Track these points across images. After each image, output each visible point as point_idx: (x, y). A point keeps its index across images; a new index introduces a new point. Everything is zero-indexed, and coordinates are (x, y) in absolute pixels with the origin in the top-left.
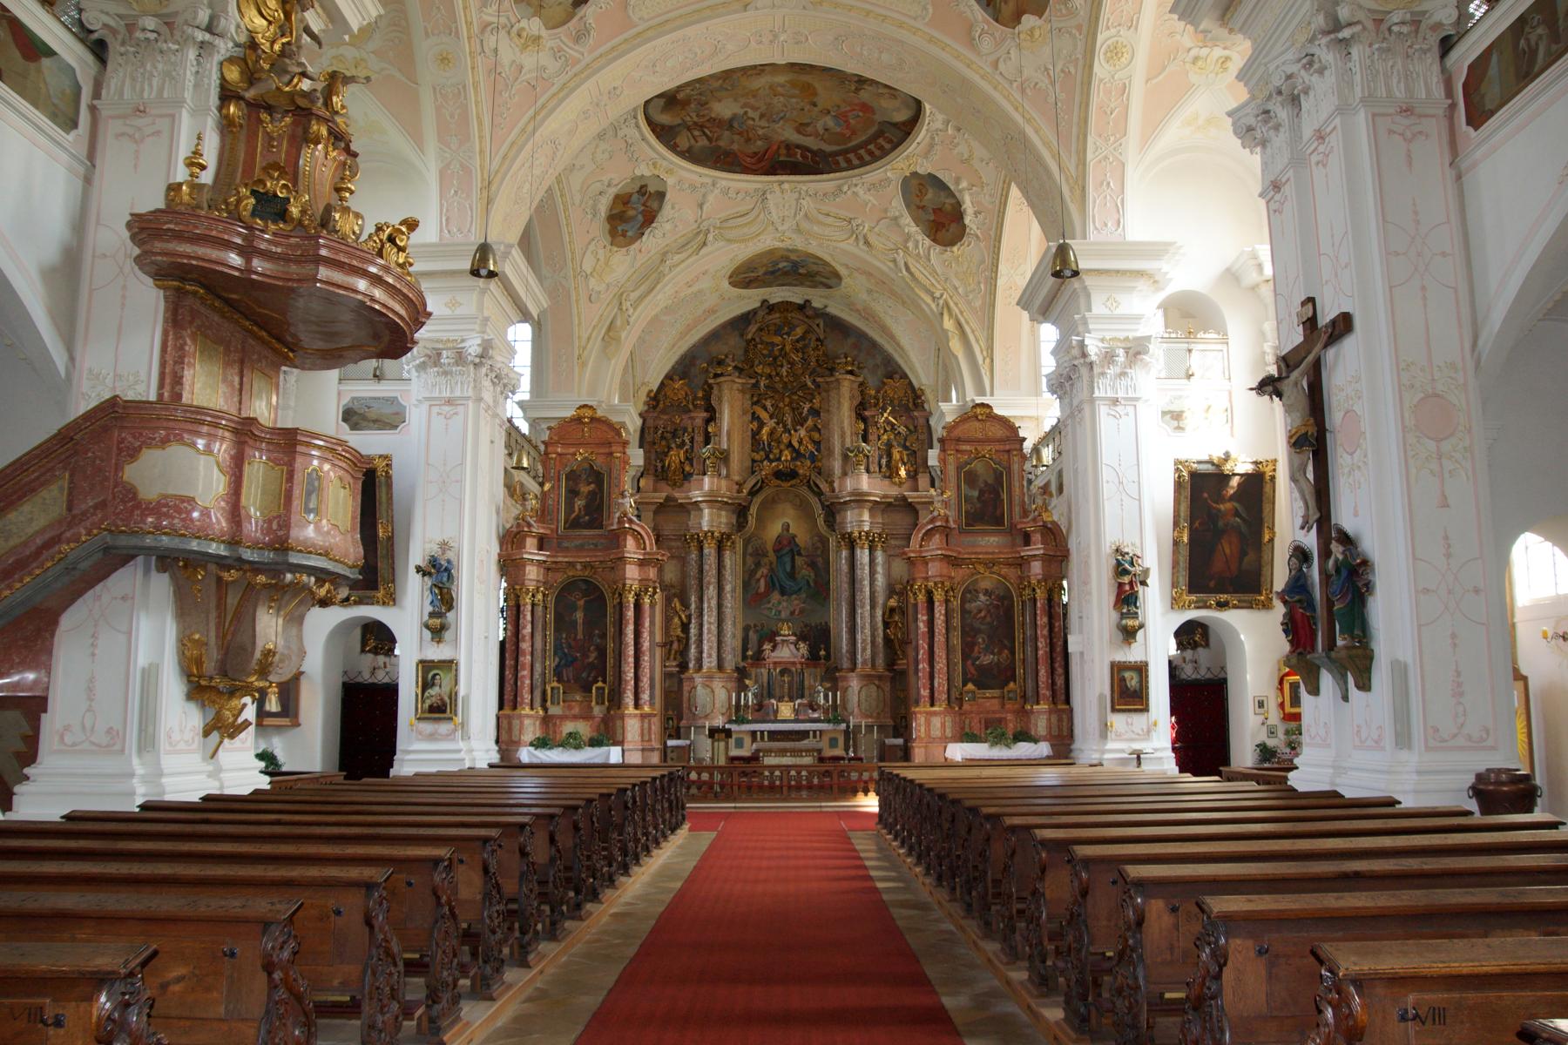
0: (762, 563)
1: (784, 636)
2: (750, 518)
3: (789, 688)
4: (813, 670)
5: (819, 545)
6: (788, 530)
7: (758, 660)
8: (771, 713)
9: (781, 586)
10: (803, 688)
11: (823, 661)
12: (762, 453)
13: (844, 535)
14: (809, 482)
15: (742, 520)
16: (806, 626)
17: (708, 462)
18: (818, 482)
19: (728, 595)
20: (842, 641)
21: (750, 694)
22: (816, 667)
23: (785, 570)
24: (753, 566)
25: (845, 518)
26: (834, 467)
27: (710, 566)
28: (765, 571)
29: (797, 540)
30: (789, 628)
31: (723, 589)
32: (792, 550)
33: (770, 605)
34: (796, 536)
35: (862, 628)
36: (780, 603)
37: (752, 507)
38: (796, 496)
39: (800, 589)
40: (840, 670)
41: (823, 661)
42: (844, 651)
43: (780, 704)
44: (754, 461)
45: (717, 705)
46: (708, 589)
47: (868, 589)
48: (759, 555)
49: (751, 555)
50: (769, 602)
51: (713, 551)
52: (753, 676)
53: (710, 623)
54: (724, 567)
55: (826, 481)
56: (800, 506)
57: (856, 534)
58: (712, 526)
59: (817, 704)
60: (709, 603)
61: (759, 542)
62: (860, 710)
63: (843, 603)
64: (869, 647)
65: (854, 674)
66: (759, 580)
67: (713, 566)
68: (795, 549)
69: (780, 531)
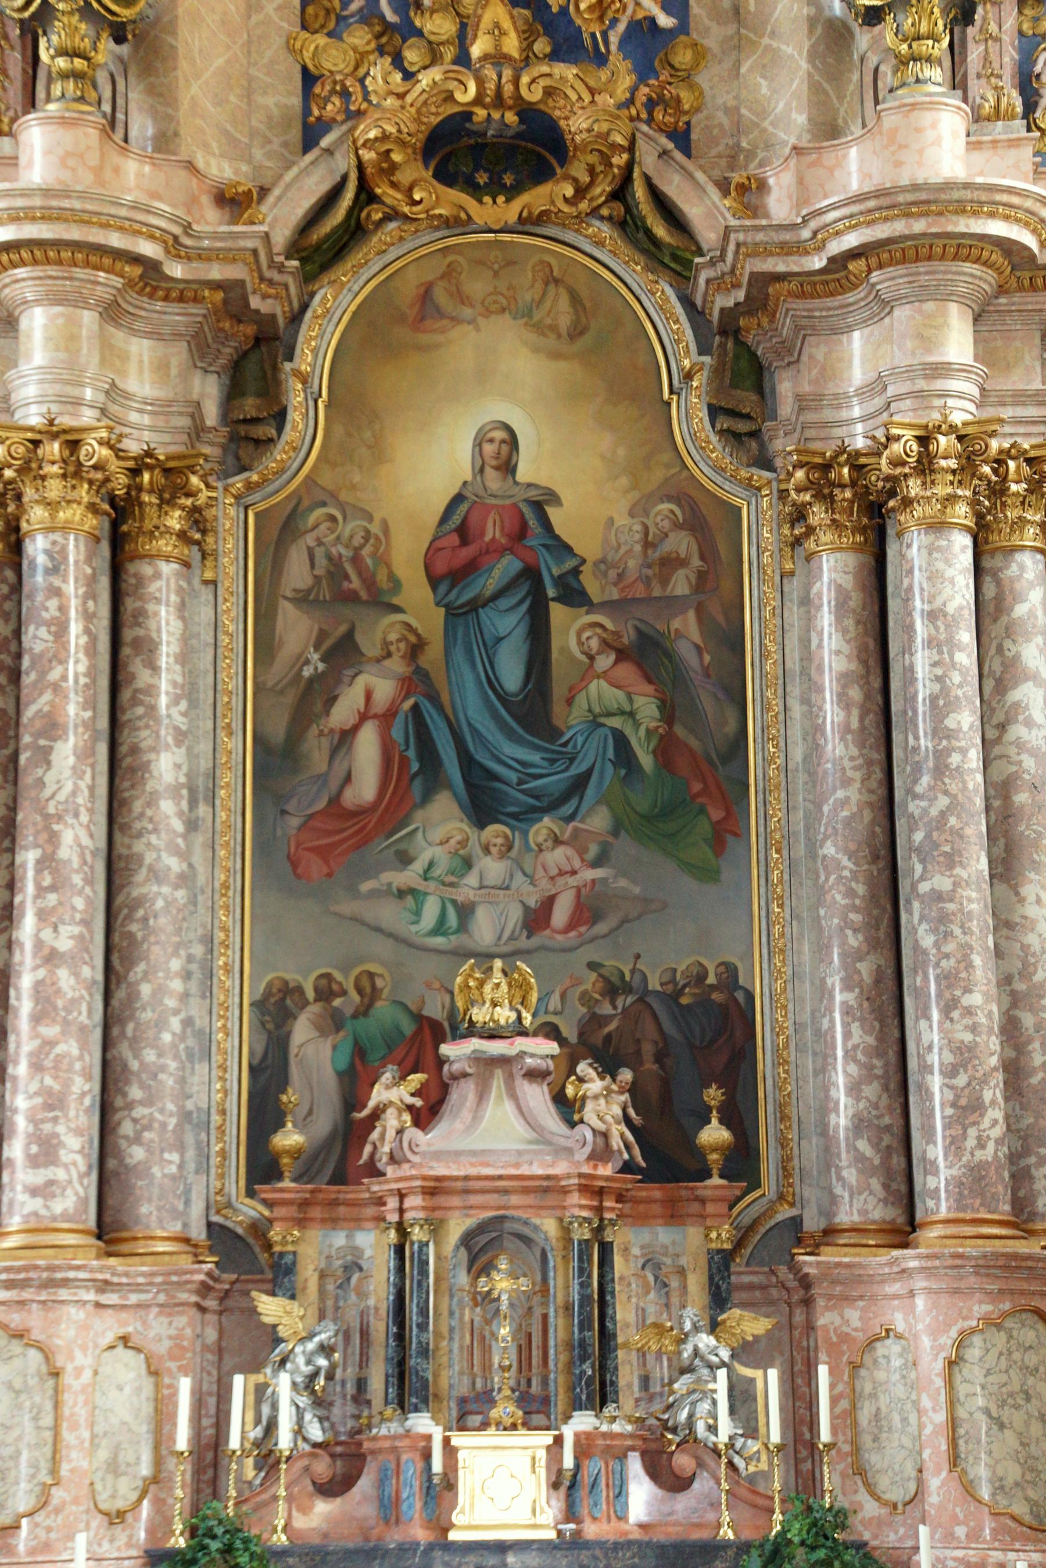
0: (369, 644)
1: (492, 1034)
2: (296, 397)
3: (524, 1349)
4: (664, 1235)
5: (682, 543)
6: (508, 468)
7: (339, 1178)
8: (413, 1505)
9: (466, 760)
10: (606, 1337)
11: (716, 1181)
12: (360, 37)
13: (826, 467)
14: (621, 193)
15: (250, 406)
16: (612, 989)
17: (44, 56)
18: (673, 187)
19: (167, 806)
20: (824, 1068)
21: (283, 1385)
22: (674, 1215)
23: (493, 683)
24: (315, 664)
25: (828, 372)
26: (763, 114)
27: (60, 629)
28: (384, 689)
29: (552, 512)
30: (519, 989)
31: (140, 771)
32: (531, 574)
33: (409, 877)
34: (553, 498)
35: (948, 979)
36: (468, 864)
37: (308, 330)
38: (552, 280)
39: (580, 783)
40: (830, 1233)
41: (716, 1181)
42: (841, 1120)
43: (458, 1439)
44: (309, 78)
45: (75, 1460)
46: (44, 756)
47: (974, 758)
48: (352, 597)
49: (303, 599)
50: (405, 859)
51: (74, 549)
52: (308, 1274)
53: (51, 958)
54: (148, 648)
55: (724, 187)
56: (577, 332)
57: (906, 445)
58: (77, 402)
59: (690, 1439)
60: (54, 839)
61: (350, 528)
62: (969, 1489)
63: (829, 849)
64: (993, 1093)
65: (910, 1258)
66: (347, 736)
67: (75, 628)
68: (552, 568)
69: (465, 470)
